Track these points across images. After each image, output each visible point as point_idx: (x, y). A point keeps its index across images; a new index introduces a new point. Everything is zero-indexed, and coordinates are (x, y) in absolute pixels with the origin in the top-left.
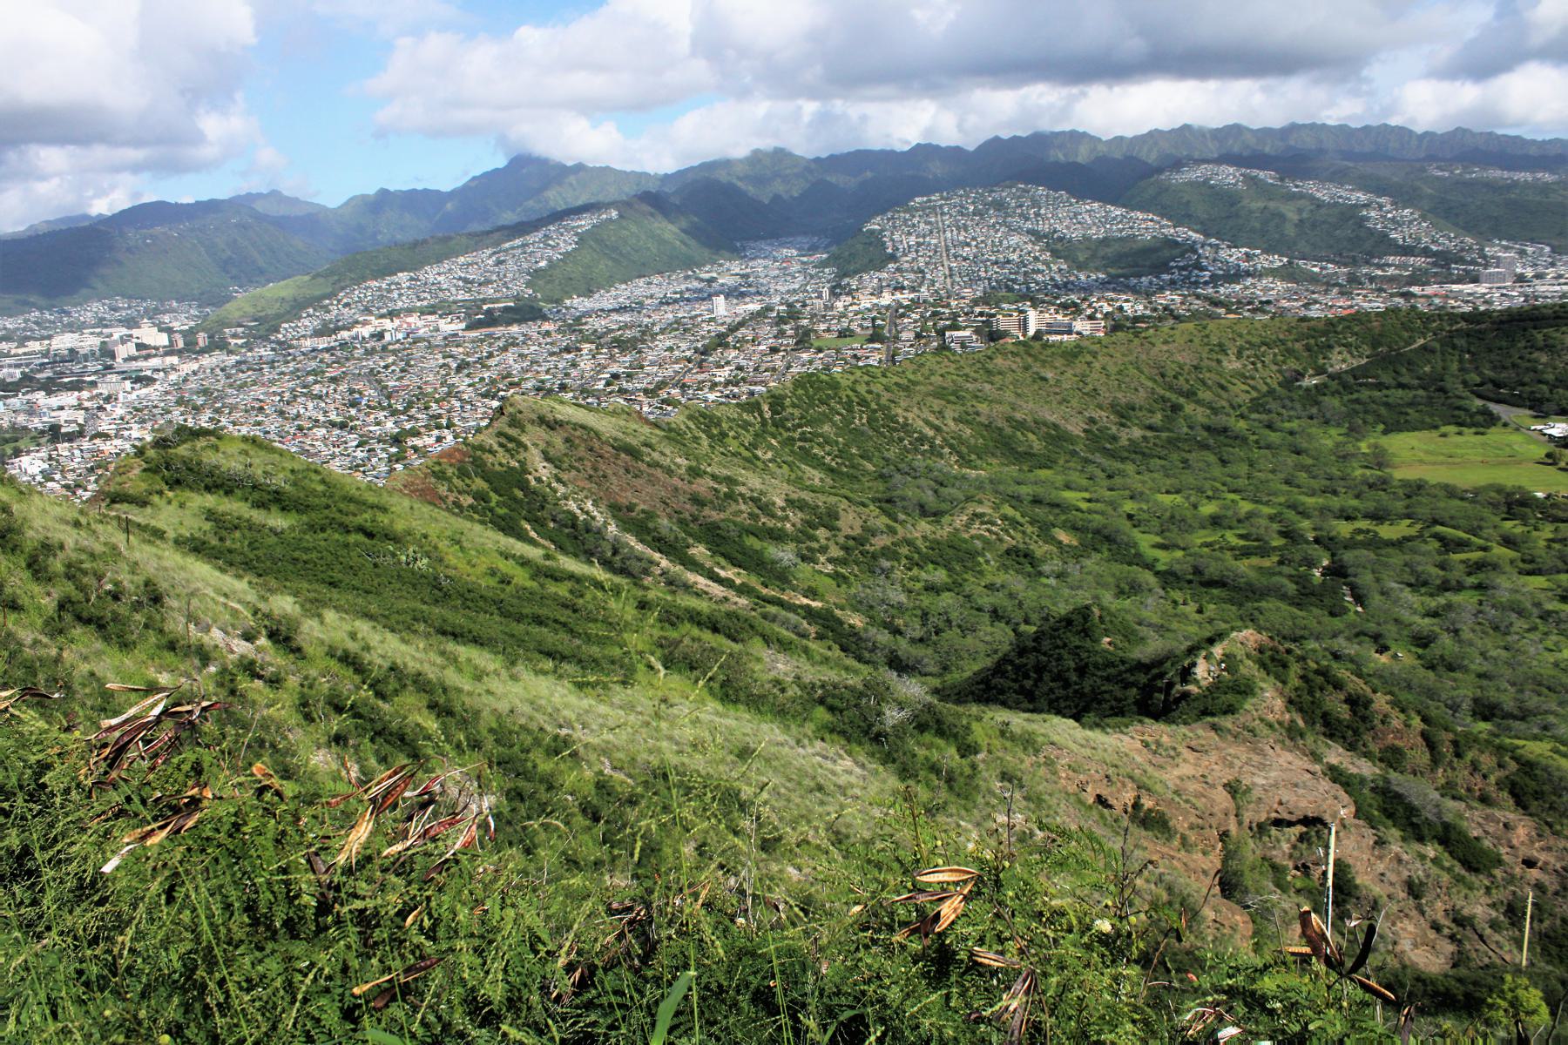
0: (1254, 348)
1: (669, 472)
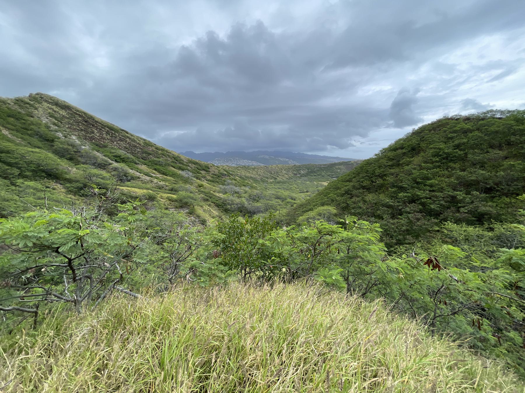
1: (134, 141)
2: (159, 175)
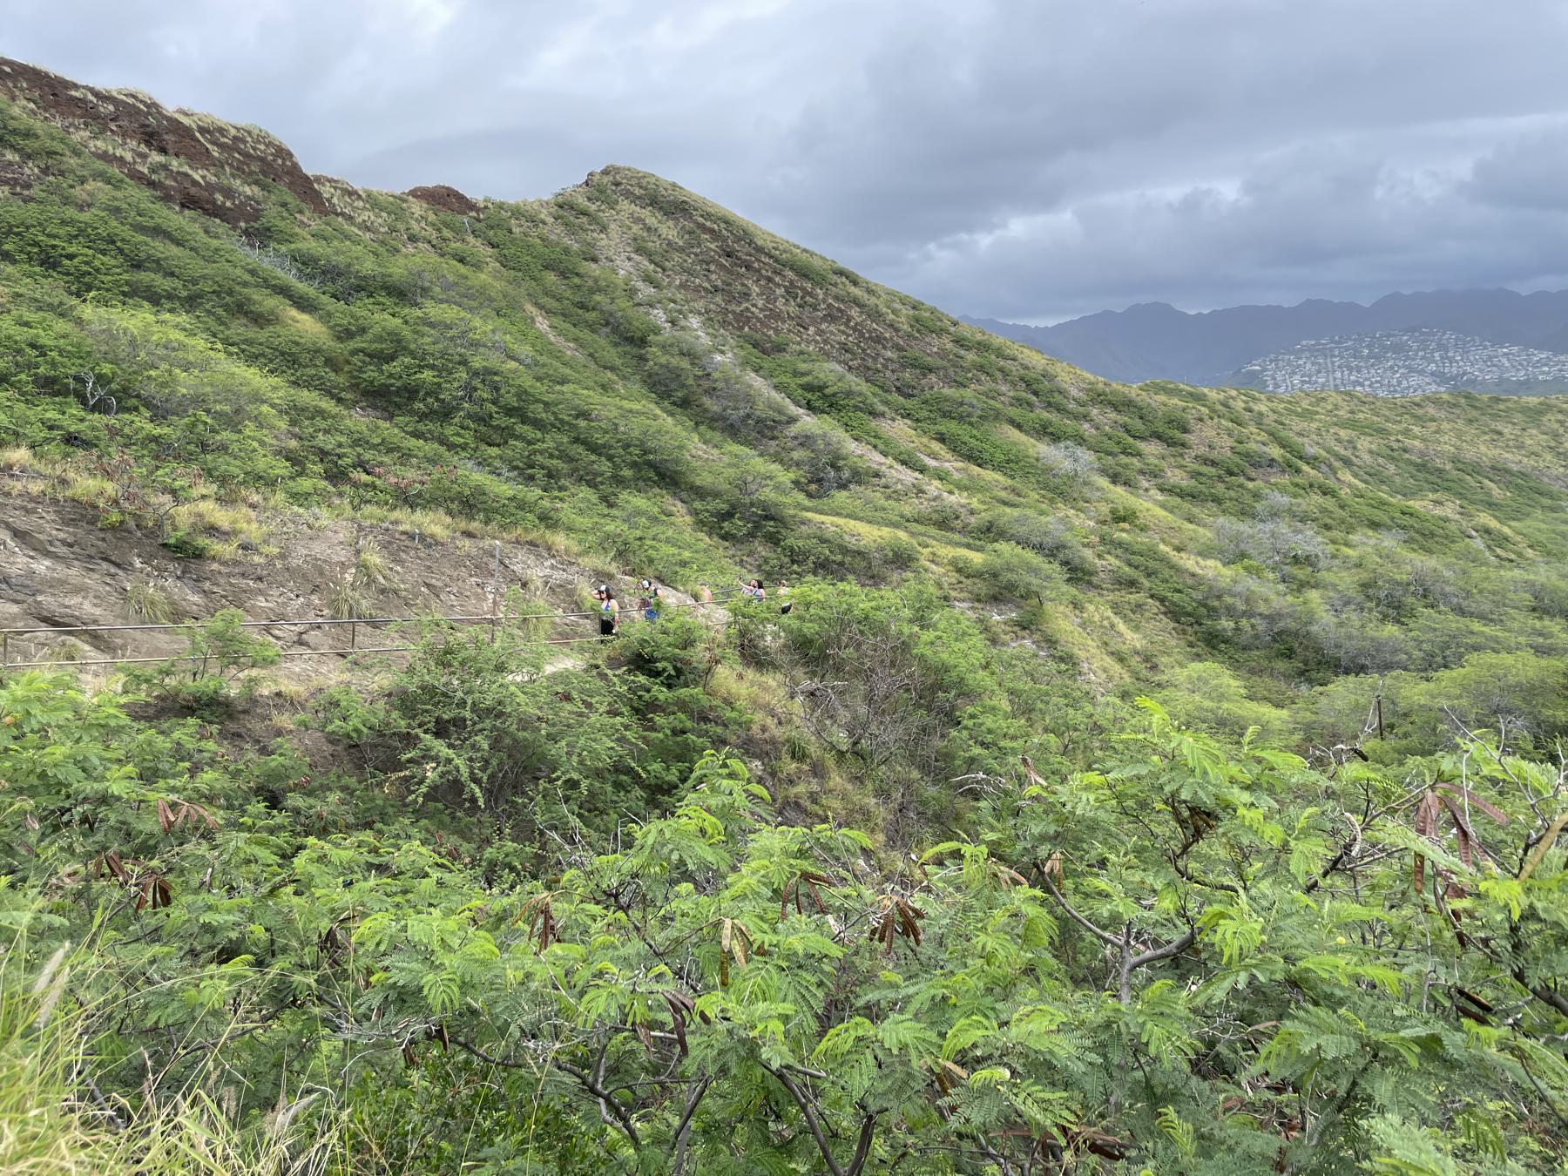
1: (875, 315)
2: (953, 465)
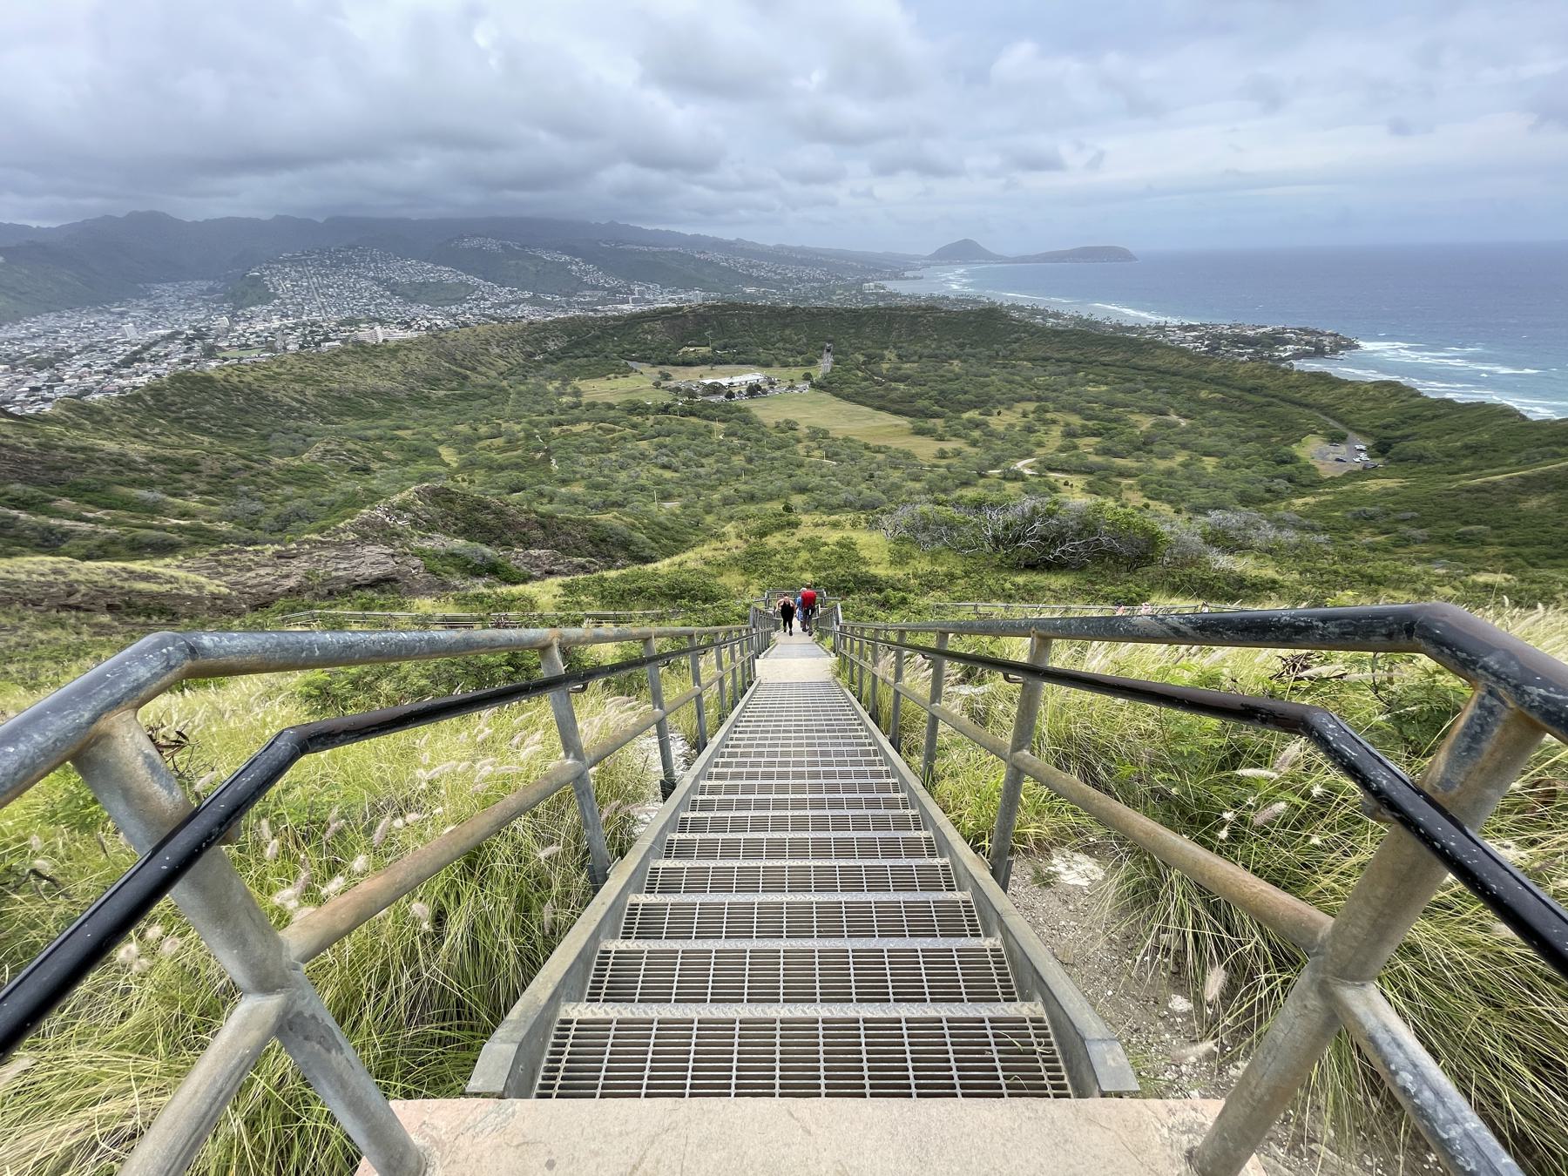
0: (506, 341)
1: (17, 449)
2: (100, 514)
